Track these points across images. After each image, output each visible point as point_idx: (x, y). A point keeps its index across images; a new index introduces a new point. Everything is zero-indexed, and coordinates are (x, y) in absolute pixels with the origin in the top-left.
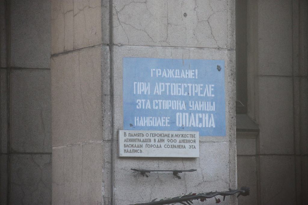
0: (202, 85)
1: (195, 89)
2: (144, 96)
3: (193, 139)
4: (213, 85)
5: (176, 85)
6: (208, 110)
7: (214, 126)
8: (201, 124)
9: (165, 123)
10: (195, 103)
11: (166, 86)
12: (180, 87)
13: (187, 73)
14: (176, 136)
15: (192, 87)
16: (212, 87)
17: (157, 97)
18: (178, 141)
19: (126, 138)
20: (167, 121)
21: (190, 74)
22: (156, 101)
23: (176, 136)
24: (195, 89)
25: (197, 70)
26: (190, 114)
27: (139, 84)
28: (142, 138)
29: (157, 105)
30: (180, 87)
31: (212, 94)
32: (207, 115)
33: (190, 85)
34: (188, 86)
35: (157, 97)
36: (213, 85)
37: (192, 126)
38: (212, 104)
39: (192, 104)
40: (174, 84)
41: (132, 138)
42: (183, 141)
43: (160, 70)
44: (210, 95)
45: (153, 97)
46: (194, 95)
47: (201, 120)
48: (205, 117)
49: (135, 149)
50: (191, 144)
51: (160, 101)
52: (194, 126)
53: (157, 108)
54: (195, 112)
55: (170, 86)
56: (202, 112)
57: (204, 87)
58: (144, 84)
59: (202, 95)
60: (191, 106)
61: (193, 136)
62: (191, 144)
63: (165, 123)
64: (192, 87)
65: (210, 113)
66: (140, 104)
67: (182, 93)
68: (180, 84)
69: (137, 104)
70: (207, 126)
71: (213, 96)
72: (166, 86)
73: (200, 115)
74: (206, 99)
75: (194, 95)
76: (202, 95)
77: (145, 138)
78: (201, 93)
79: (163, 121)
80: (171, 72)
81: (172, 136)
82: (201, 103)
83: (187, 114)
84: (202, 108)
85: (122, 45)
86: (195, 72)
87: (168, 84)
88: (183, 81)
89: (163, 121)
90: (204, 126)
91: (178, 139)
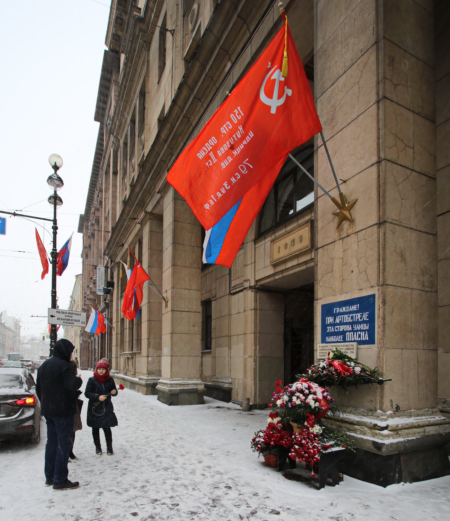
0: (361, 314)
1: (357, 317)
2: (330, 325)
3: (352, 347)
4: (368, 313)
5: (346, 316)
6: (364, 329)
7: (367, 339)
8: (360, 338)
9: (340, 339)
10: (357, 326)
11: (341, 317)
12: (349, 317)
13: (353, 307)
14: (343, 346)
15: (355, 315)
16: (367, 314)
17: (337, 324)
18: (344, 349)
19: (320, 349)
20: (342, 338)
21: (354, 308)
22: (337, 327)
23: (343, 346)
24: (357, 317)
25: (358, 305)
26: (354, 334)
27: (328, 318)
28: (327, 348)
29: (337, 329)
30: (349, 317)
31: (367, 318)
32: (364, 332)
33: (354, 315)
34: (353, 316)
35: (337, 324)
36: (368, 313)
37: (355, 340)
38: (367, 325)
39: (355, 327)
40: (346, 315)
41: (323, 348)
42: (347, 349)
43: (339, 308)
44: (366, 319)
45: (334, 325)
46: (356, 320)
47: (360, 336)
48: (362, 334)
49: (324, 354)
50: (351, 351)
51: (339, 326)
52: (356, 340)
53: (337, 331)
54: (357, 331)
55: (343, 317)
56: (361, 331)
57: (362, 315)
58: (331, 318)
59: (361, 320)
60: (354, 328)
61: (352, 345)
62: (351, 351)
63: (340, 339)
64: (355, 315)
65: (365, 331)
66: (329, 329)
67: (350, 320)
68: (349, 315)
69: (327, 329)
70: (363, 340)
71: (368, 319)
72: (341, 317)
73: (360, 332)
74: (364, 322)
75: (356, 320)
76: (361, 320)
77: (328, 348)
78: (360, 319)
79: (339, 338)
80: (344, 308)
81: (341, 346)
82: (361, 325)
83: (352, 333)
84: (360, 328)
85: (321, 299)
86: (357, 306)
87: (342, 316)
88: (350, 313)
89: (339, 338)
90: (361, 340)
91: (344, 348)
